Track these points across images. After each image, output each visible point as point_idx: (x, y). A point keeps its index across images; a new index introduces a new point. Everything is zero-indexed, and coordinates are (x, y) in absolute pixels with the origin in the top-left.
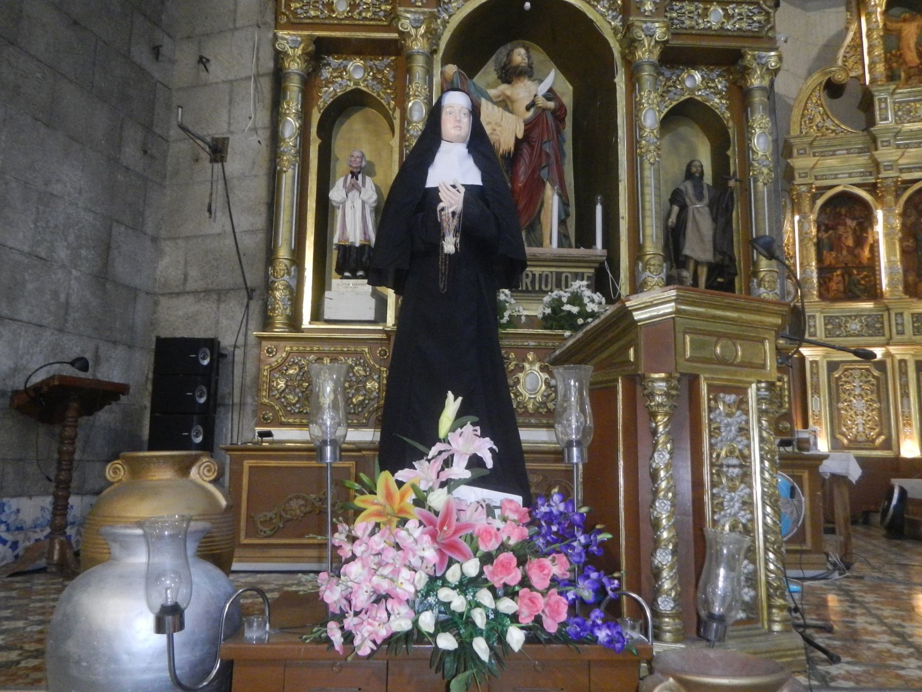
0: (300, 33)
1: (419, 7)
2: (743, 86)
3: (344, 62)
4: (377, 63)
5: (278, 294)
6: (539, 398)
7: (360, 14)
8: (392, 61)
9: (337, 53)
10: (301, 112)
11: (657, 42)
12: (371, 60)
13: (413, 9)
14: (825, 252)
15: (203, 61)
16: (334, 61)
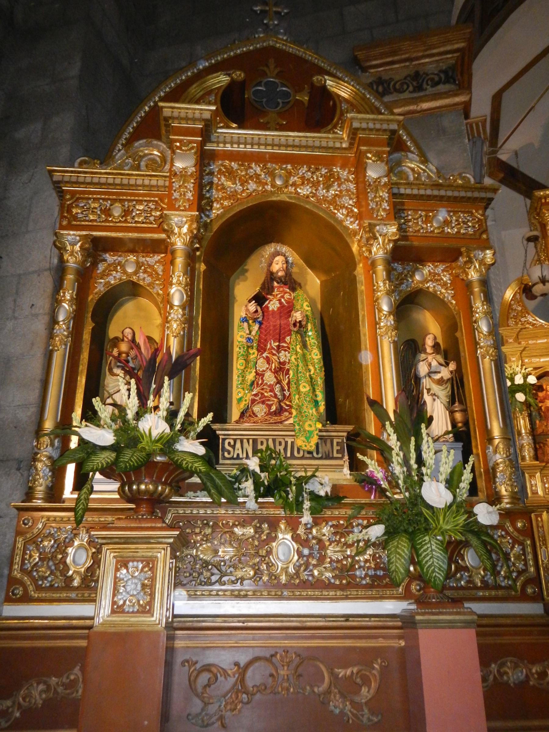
0: (79, 233)
1: (183, 210)
2: (465, 278)
3: (119, 259)
4: (148, 259)
5: (39, 465)
6: (291, 570)
7: (133, 218)
8: (162, 258)
9: (113, 251)
10: (76, 299)
11: (389, 241)
12: (143, 257)
13: (177, 213)
14: (538, 422)
16: (110, 258)
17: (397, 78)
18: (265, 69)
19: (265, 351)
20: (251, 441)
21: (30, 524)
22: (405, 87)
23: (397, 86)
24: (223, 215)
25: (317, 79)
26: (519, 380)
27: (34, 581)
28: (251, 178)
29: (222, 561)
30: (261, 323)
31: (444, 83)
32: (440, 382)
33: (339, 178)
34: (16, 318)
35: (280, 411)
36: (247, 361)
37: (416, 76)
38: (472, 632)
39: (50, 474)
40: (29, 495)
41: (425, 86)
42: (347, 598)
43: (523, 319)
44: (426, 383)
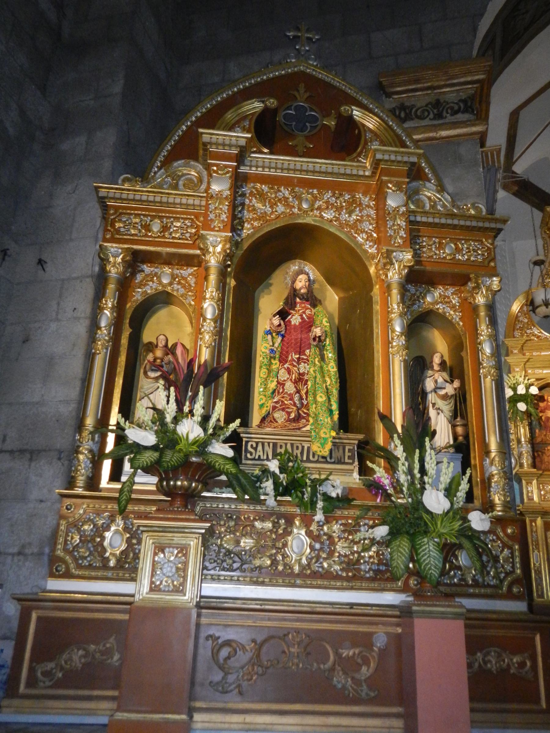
0: (121, 246)
1: (217, 231)
2: (473, 302)
3: (156, 270)
4: (182, 272)
5: (81, 457)
6: (304, 561)
7: (171, 234)
8: (195, 271)
9: (150, 262)
10: (117, 307)
11: (404, 266)
12: (178, 269)
13: (212, 233)
14: (537, 431)
15: (41, 262)
16: (147, 269)
17: (419, 105)
18: (296, 93)
19: (286, 362)
20: (271, 445)
21: (72, 509)
22: (426, 113)
23: (419, 113)
24: (253, 234)
25: (345, 109)
26: (521, 390)
27: (75, 560)
28: (280, 200)
29: (243, 551)
30: (283, 336)
31: (463, 112)
32: (445, 397)
33: (361, 204)
34: (57, 320)
35: (298, 418)
36: (269, 371)
37: (437, 104)
38: (460, 624)
39: (91, 465)
40: (71, 483)
41: (444, 114)
42: (352, 588)
43: (528, 331)
44: (431, 397)
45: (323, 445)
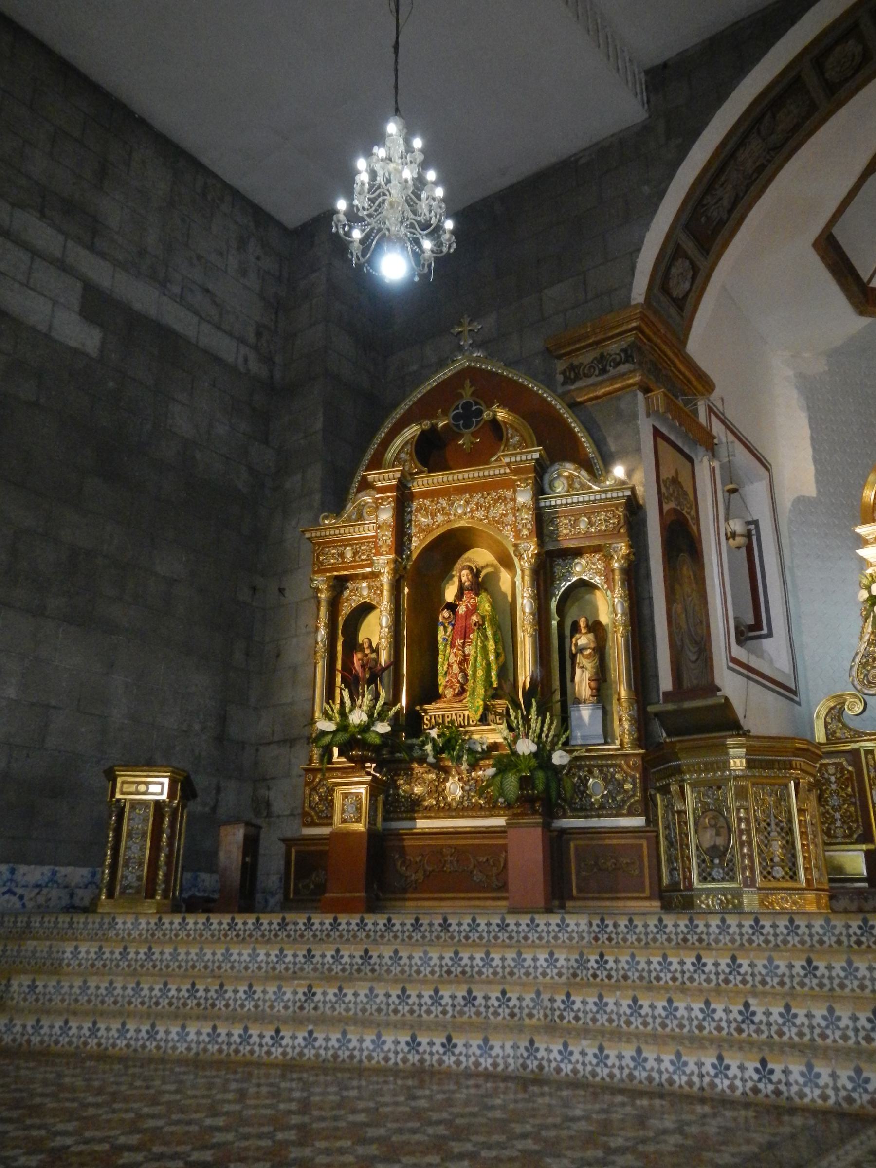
15: (281, 591)
17: (586, 362)
24: (419, 545)
27: (317, 813)
28: (439, 511)
30: (453, 625)
33: (505, 498)
34: (296, 635)
41: (608, 368)
42: (492, 816)
45: (476, 712)
